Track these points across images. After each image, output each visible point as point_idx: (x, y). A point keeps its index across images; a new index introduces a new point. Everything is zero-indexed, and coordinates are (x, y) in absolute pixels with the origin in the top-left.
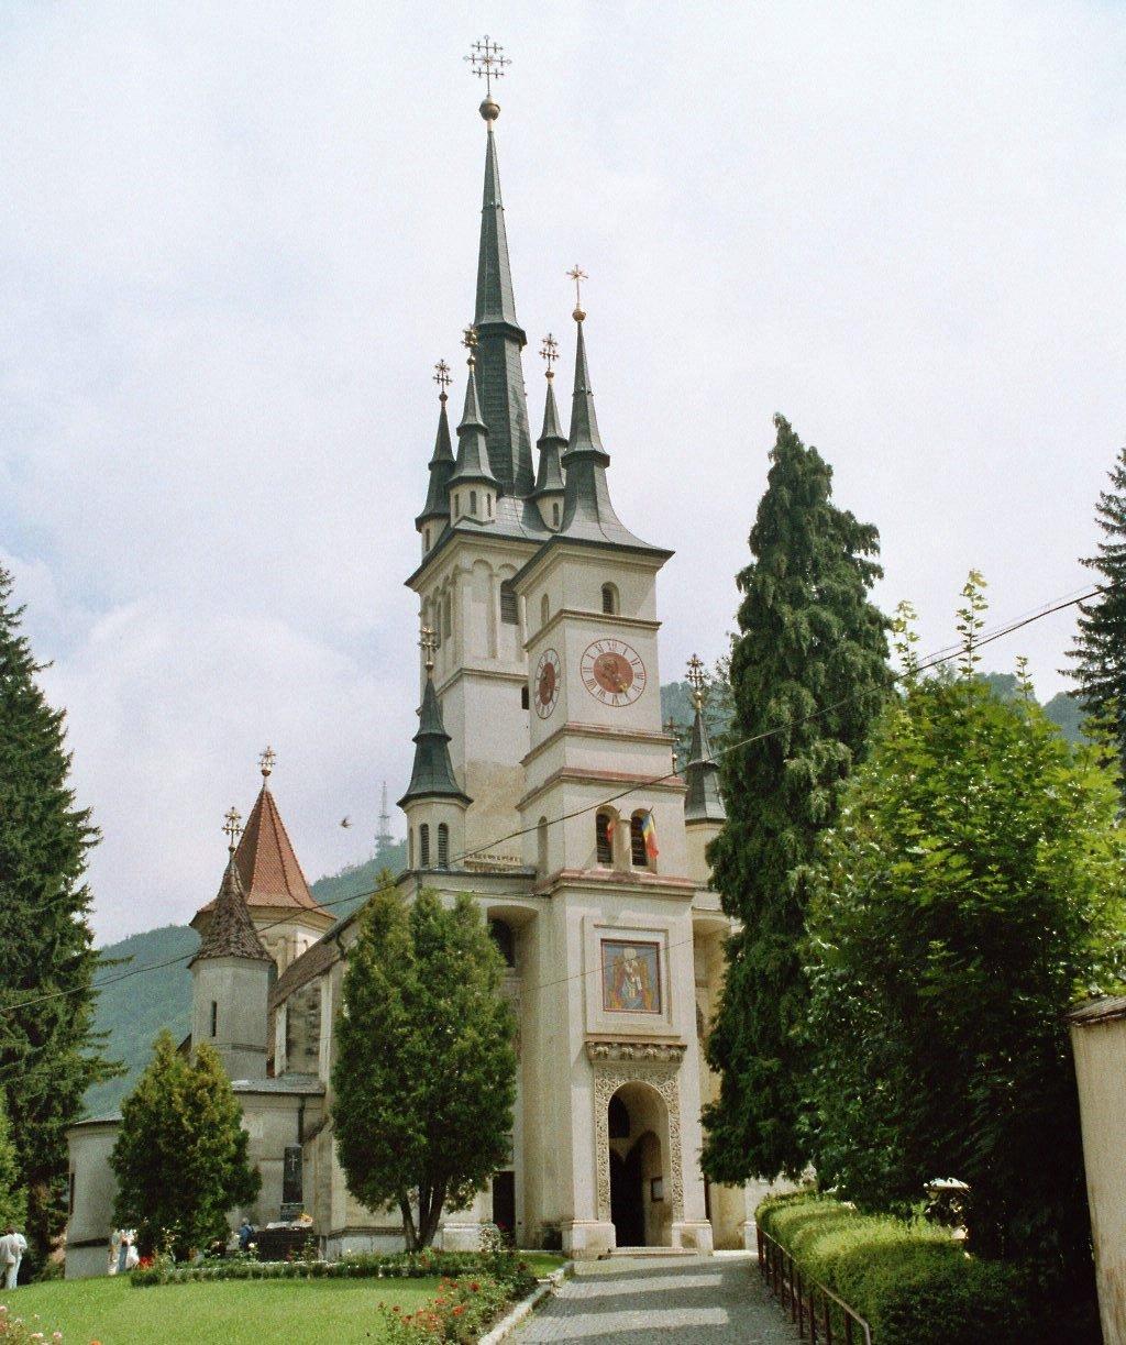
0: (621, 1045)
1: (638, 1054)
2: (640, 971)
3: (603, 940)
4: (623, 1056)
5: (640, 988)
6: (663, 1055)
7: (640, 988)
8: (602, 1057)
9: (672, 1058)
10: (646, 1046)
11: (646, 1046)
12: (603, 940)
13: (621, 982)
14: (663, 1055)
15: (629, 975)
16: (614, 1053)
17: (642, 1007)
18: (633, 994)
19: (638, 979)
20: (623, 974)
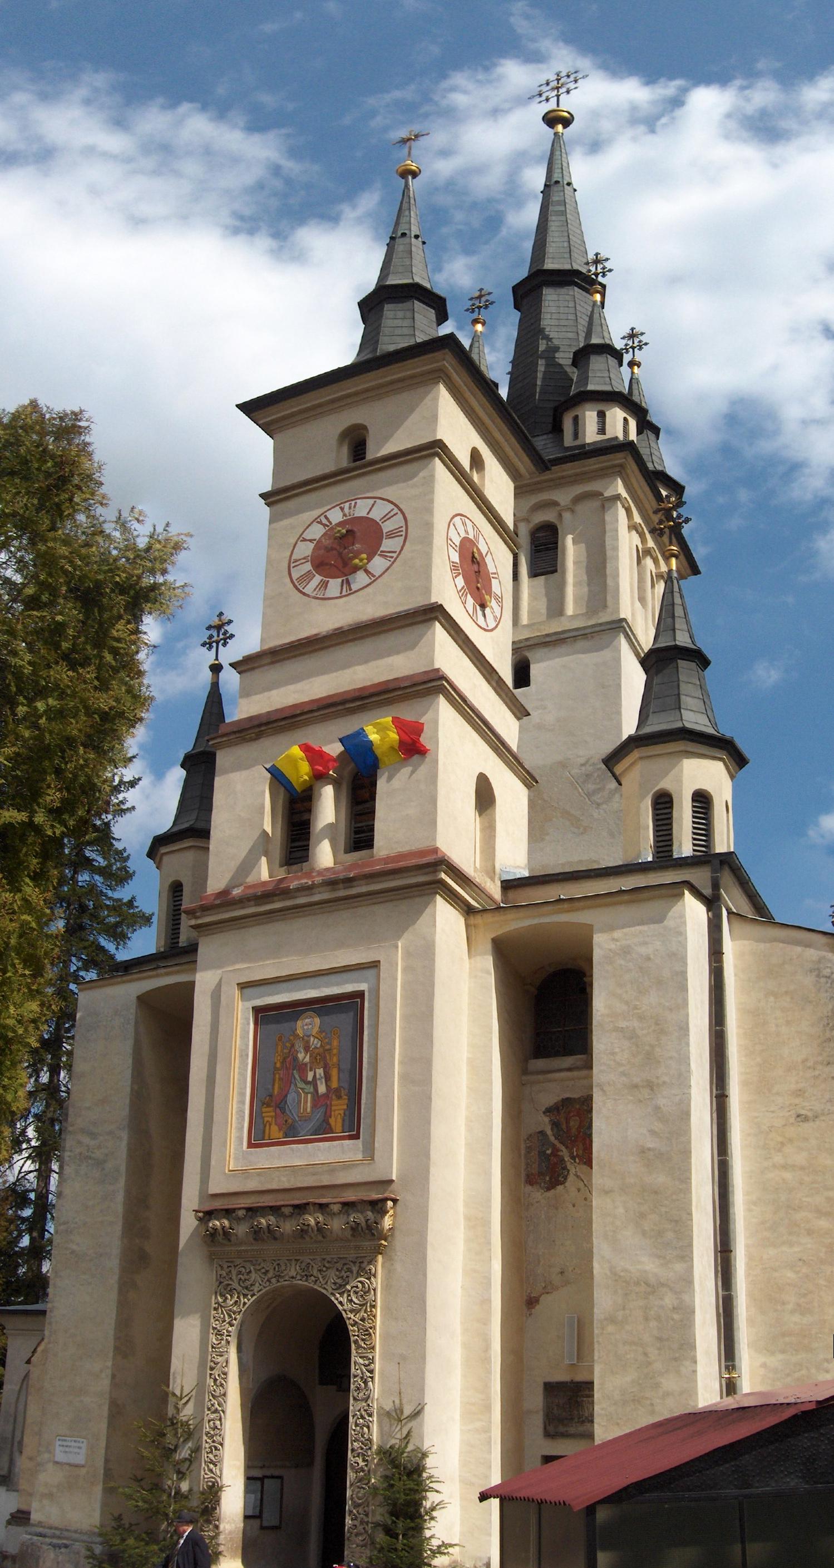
0: (252, 1211)
1: (288, 1227)
2: (320, 1058)
3: (257, 1010)
4: (257, 1233)
5: (322, 1089)
6: (337, 1225)
7: (322, 1089)
8: (220, 1238)
9: (355, 1229)
10: (301, 1209)
11: (301, 1209)
12: (257, 1010)
13: (288, 1082)
14: (337, 1225)
15: (302, 1068)
16: (242, 1230)
17: (323, 1131)
18: (308, 1104)
19: (320, 1072)
20: (291, 1066)
